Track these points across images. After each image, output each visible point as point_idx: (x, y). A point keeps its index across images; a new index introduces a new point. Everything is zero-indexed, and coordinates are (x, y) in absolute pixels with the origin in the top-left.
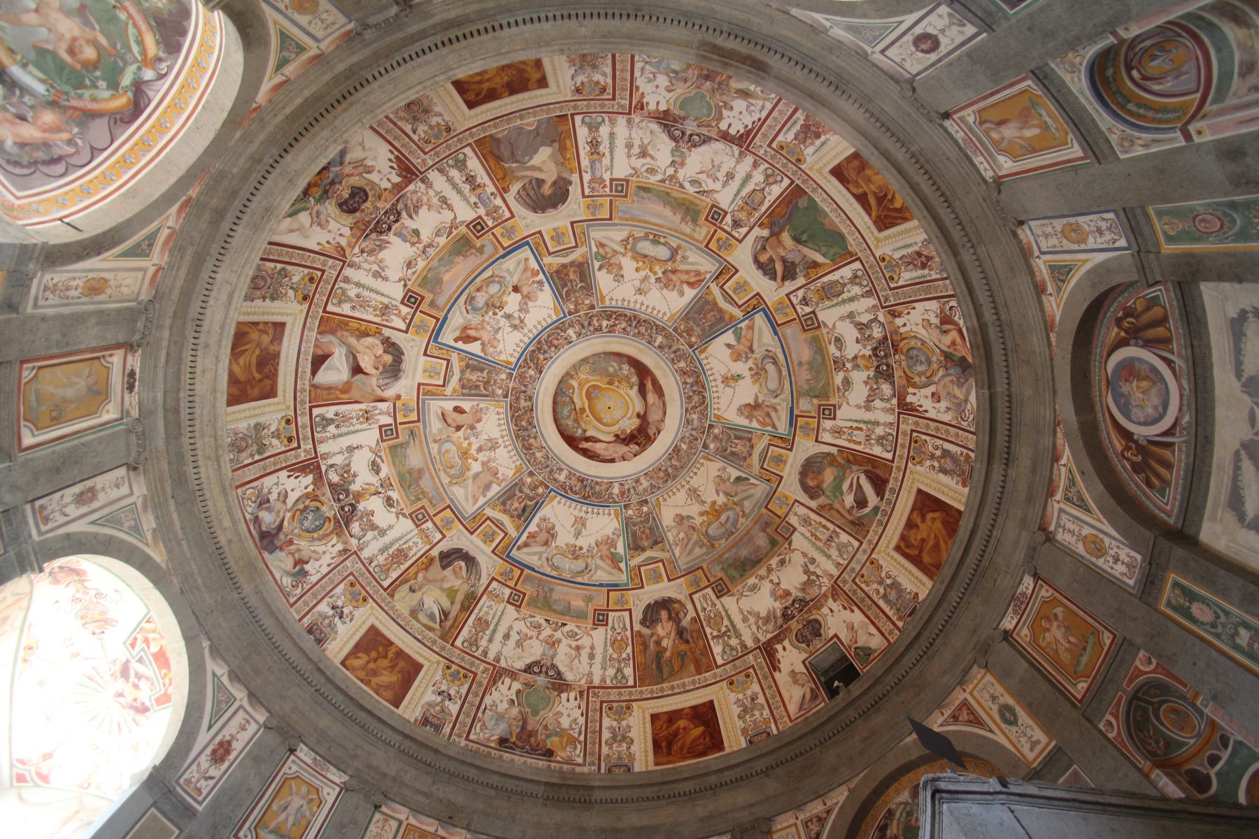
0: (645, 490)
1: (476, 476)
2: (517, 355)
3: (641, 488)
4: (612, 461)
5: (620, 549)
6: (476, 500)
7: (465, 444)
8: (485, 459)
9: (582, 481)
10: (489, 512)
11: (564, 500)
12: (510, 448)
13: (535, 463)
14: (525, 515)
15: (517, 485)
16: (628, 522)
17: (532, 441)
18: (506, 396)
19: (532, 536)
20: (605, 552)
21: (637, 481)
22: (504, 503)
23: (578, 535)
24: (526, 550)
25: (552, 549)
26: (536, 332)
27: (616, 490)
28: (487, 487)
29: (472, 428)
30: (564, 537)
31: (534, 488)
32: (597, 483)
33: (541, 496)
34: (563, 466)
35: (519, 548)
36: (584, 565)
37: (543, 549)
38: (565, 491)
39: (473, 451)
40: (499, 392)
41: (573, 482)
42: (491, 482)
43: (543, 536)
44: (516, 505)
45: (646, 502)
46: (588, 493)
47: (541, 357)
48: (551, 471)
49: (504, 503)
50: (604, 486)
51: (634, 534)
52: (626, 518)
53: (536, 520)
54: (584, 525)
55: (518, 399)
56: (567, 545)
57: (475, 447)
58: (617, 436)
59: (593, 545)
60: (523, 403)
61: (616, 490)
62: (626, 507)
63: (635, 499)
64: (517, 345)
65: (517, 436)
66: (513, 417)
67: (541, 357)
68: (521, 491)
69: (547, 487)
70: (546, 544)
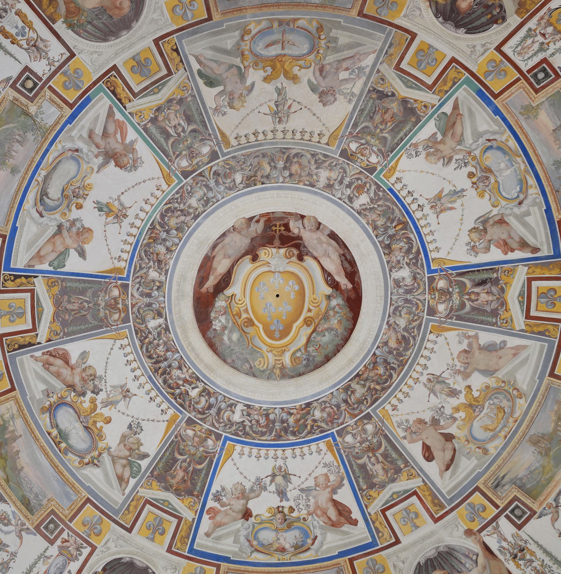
0: (331, 168)
1: (488, 372)
2: (313, 446)
3: (334, 175)
4: (333, 236)
5: (429, 129)
6: (517, 350)
7: (461, 415)
8: (459, 378)
9: (388, 247)
10: (520, 322)
11: (430, 247)
12: (422, 361)
13: (415, 317)
14: (487, 277)
15: (458, 315)
16: (389, 151)
17: (393, 344)
18: (368, 417)
19: (506, 247)
20: (450, 143)
21: (329, 186)
22: (495, 313)
23: (457, 194)
24: (531, 240)
25: (504, 208)
26: (271, 452)
27: (363, 199)
28: (491, 348)
29: (435, 422)
30: (477, 206)
31: (445, 293)
32: (375, 228)
33: (447, 277)
34: (391, 283)
35: (536, 250)
36: (489, 154)
37: (511, 220)
38: (418, 255)
39: (462, 399)
40: (370, 428)
41: (398, 256)
42: (481, 348)
43: (495, 233)
44: (484, 297)
45: (344, 154)
46: (397, 226)
47: (291, 420)
48: (408, 292)
49: (495, 313)
50: (373, 216)
51: (395, 131)
52: (385, 156)
53: (483, 258)
54: (439, 197)
55: (360, 402)
56: (481, 195)
57: (454, 402)
58: (300, 258)
59: (453, 165)
60: (360, 391)
61: (363, 199)
62: (371, 170)
63: (353, 169)
64: (303, 456)
65: (402, 364)
66: (384, 389)
67: (291, 420)
68: (463, 305)
69: (432, 280)
70: (502, 222)
